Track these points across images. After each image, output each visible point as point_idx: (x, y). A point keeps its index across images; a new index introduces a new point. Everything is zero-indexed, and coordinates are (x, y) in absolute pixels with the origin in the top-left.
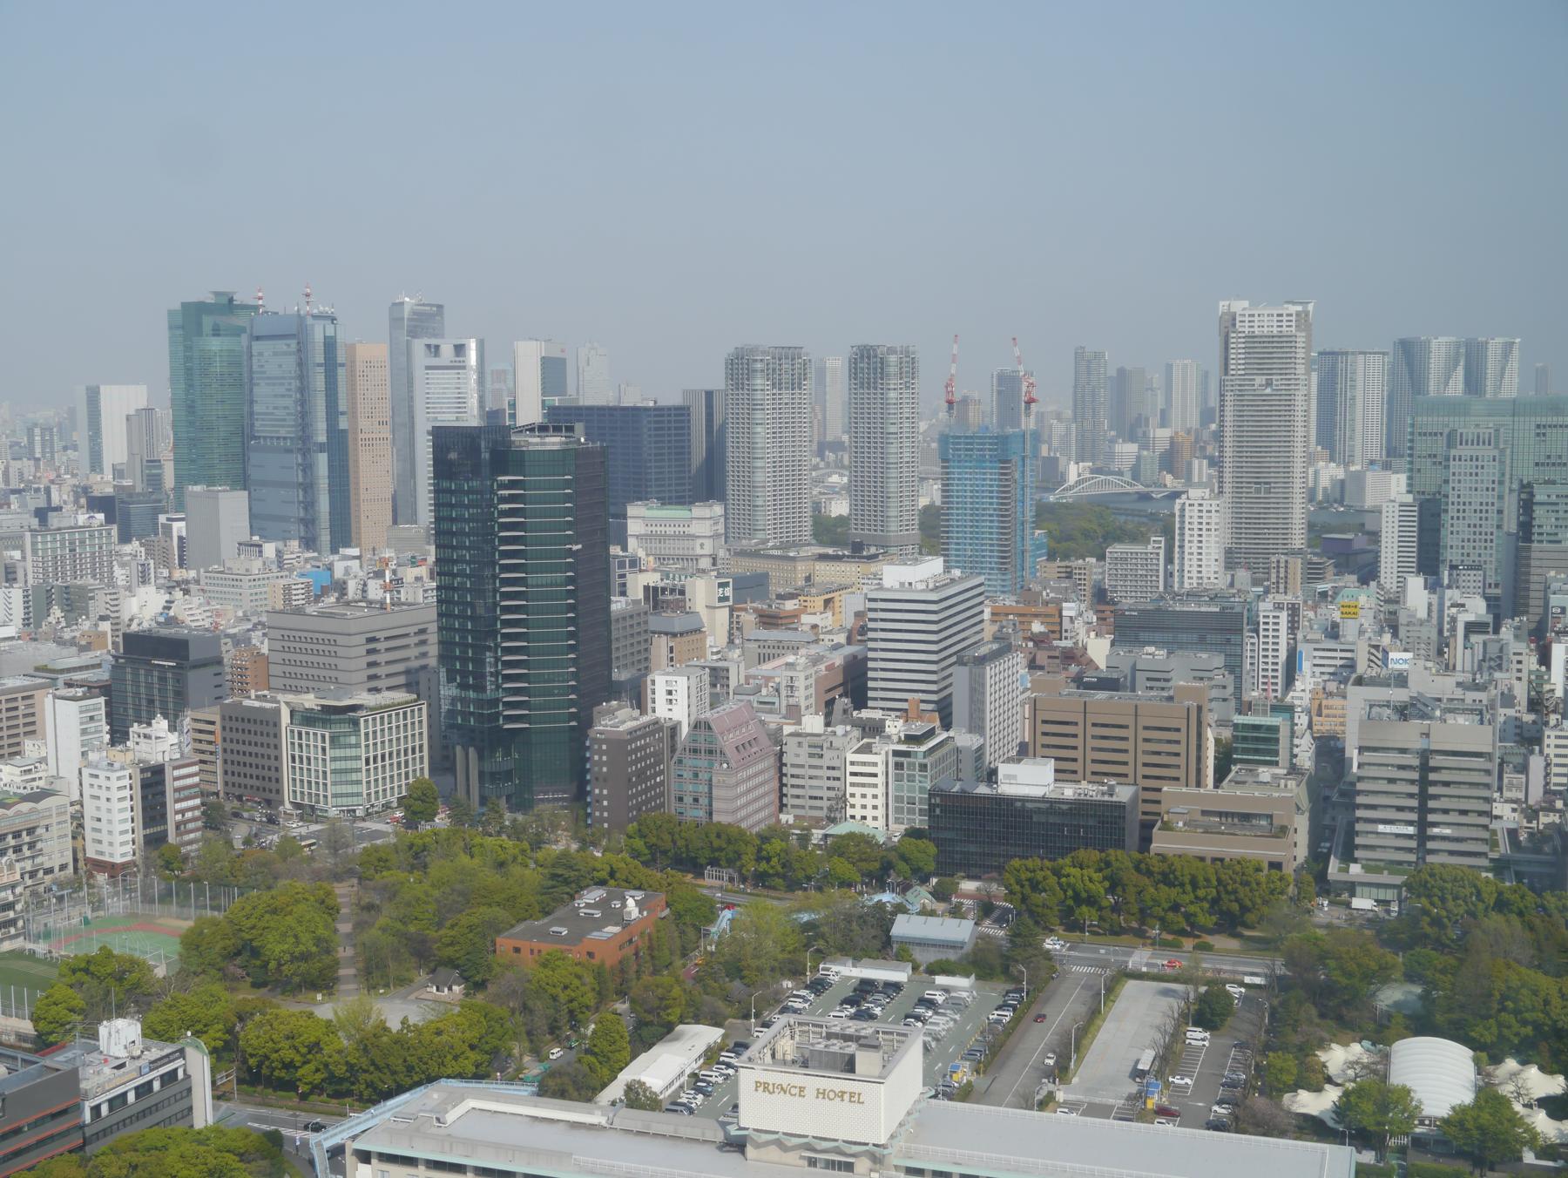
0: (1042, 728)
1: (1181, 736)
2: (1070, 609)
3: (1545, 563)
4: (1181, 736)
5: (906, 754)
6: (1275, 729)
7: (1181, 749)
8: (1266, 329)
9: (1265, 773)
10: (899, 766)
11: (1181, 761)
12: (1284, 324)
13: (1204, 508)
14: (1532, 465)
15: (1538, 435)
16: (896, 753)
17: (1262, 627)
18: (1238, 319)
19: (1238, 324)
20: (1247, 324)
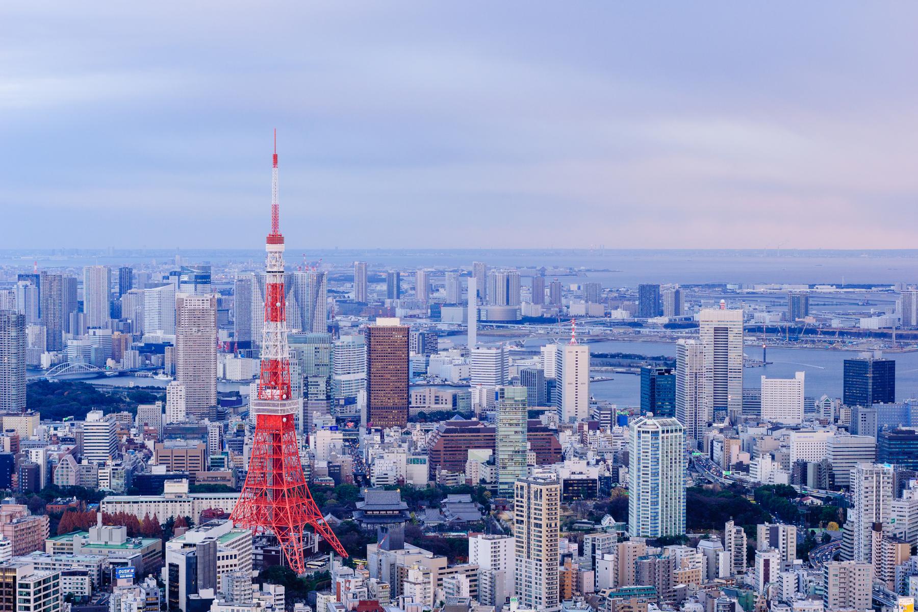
0: (159, 458)
1: (200, 458)
2: (133, 431)
3: (314, 409)
4: (200, 458)
5: (117, 469)
6: (223, 459)
7: (200, 462)
8: (197, 306)
9: (222, 469)
10: (114, 473)
11: (200, 465)
12: (205, 304)
13: (179, 389)
14: (314, 365)
15: (316, 352)
16: (113, 469)
17: (210, 433)
18: (185, 302)
19: (185, 304)
20: (188, 304)
